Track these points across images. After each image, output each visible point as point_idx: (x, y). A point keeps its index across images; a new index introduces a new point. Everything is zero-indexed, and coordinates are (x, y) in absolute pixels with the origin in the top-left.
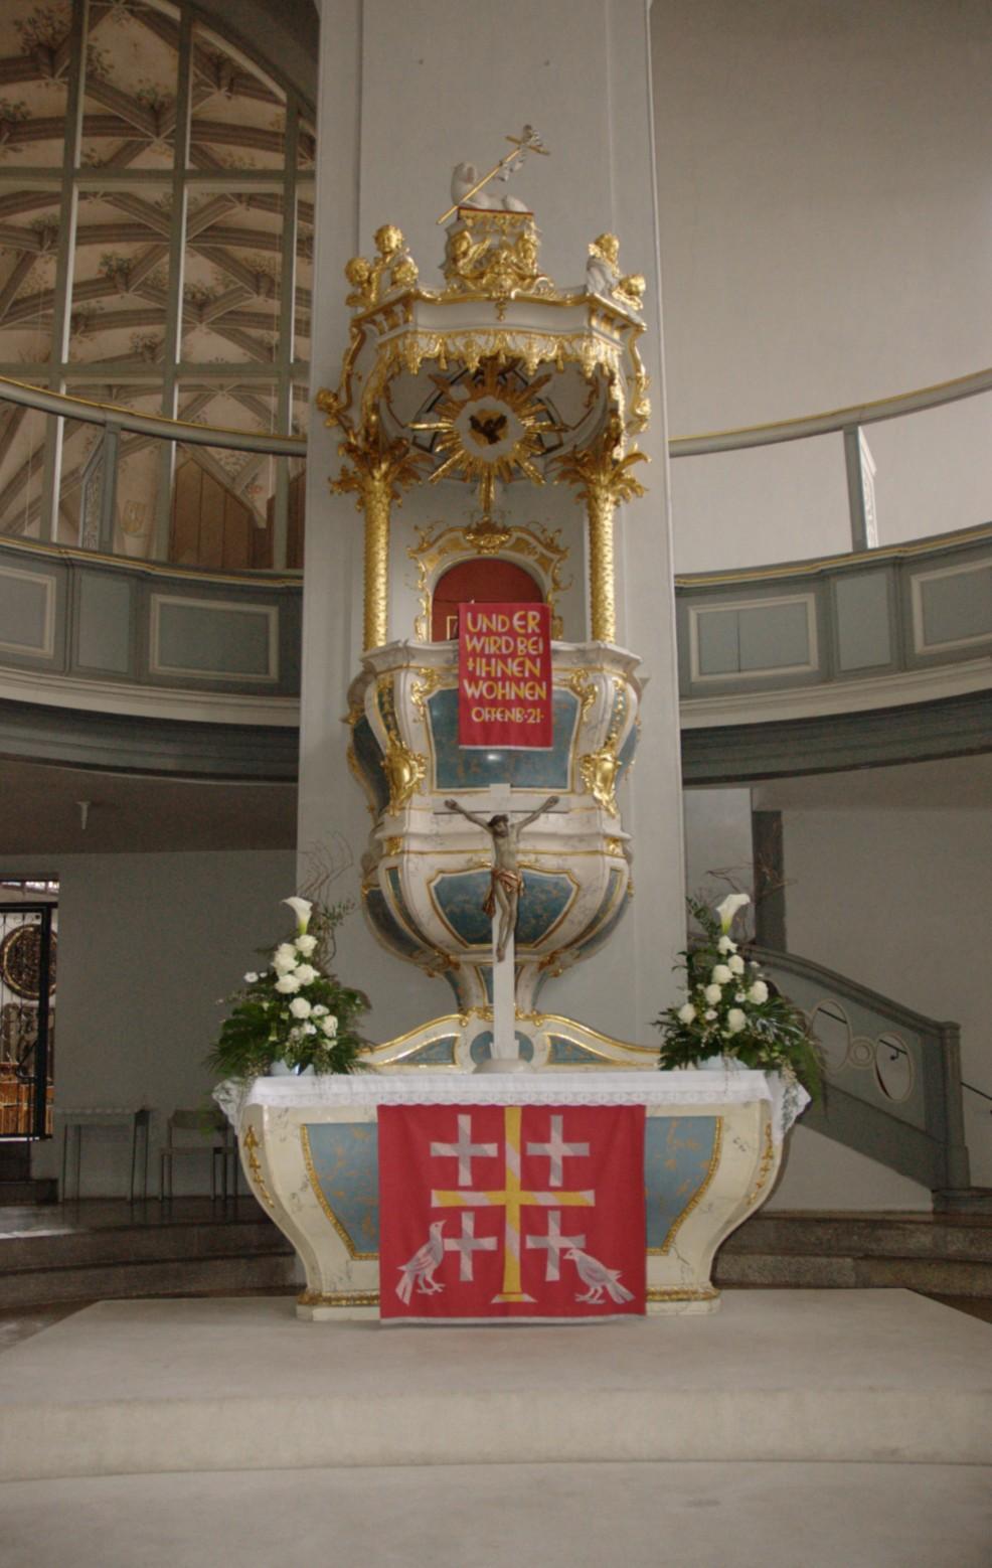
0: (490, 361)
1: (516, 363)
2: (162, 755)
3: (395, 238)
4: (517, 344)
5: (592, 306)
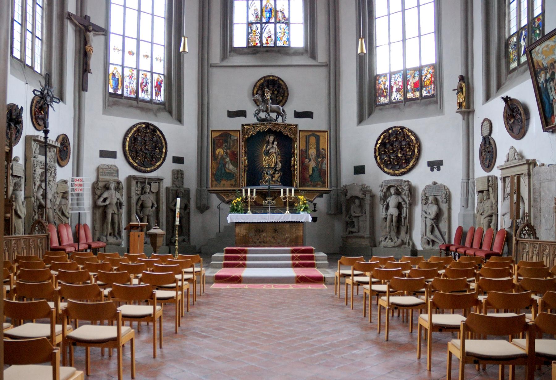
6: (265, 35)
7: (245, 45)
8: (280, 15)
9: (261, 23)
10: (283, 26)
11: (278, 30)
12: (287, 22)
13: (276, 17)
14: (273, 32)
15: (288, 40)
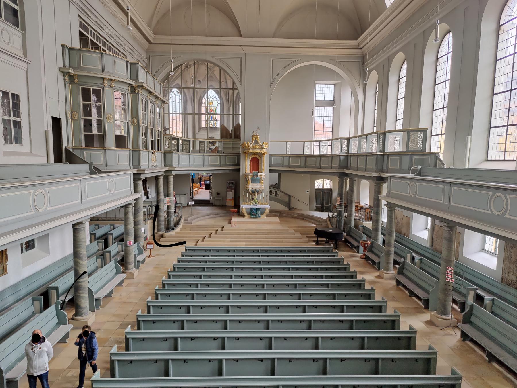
0: (255, 152)
1: (257, 152)
2: (228, 172)
3: (249, 142)
6: (210, 124)
7: (205, 127)
8: (215, 118)
9: (209, 120)
10: (215, 121)
11: (214, 123)
12: (217, 120)
13: (213, 119)
14: (213, 123)
15: (217, 125)
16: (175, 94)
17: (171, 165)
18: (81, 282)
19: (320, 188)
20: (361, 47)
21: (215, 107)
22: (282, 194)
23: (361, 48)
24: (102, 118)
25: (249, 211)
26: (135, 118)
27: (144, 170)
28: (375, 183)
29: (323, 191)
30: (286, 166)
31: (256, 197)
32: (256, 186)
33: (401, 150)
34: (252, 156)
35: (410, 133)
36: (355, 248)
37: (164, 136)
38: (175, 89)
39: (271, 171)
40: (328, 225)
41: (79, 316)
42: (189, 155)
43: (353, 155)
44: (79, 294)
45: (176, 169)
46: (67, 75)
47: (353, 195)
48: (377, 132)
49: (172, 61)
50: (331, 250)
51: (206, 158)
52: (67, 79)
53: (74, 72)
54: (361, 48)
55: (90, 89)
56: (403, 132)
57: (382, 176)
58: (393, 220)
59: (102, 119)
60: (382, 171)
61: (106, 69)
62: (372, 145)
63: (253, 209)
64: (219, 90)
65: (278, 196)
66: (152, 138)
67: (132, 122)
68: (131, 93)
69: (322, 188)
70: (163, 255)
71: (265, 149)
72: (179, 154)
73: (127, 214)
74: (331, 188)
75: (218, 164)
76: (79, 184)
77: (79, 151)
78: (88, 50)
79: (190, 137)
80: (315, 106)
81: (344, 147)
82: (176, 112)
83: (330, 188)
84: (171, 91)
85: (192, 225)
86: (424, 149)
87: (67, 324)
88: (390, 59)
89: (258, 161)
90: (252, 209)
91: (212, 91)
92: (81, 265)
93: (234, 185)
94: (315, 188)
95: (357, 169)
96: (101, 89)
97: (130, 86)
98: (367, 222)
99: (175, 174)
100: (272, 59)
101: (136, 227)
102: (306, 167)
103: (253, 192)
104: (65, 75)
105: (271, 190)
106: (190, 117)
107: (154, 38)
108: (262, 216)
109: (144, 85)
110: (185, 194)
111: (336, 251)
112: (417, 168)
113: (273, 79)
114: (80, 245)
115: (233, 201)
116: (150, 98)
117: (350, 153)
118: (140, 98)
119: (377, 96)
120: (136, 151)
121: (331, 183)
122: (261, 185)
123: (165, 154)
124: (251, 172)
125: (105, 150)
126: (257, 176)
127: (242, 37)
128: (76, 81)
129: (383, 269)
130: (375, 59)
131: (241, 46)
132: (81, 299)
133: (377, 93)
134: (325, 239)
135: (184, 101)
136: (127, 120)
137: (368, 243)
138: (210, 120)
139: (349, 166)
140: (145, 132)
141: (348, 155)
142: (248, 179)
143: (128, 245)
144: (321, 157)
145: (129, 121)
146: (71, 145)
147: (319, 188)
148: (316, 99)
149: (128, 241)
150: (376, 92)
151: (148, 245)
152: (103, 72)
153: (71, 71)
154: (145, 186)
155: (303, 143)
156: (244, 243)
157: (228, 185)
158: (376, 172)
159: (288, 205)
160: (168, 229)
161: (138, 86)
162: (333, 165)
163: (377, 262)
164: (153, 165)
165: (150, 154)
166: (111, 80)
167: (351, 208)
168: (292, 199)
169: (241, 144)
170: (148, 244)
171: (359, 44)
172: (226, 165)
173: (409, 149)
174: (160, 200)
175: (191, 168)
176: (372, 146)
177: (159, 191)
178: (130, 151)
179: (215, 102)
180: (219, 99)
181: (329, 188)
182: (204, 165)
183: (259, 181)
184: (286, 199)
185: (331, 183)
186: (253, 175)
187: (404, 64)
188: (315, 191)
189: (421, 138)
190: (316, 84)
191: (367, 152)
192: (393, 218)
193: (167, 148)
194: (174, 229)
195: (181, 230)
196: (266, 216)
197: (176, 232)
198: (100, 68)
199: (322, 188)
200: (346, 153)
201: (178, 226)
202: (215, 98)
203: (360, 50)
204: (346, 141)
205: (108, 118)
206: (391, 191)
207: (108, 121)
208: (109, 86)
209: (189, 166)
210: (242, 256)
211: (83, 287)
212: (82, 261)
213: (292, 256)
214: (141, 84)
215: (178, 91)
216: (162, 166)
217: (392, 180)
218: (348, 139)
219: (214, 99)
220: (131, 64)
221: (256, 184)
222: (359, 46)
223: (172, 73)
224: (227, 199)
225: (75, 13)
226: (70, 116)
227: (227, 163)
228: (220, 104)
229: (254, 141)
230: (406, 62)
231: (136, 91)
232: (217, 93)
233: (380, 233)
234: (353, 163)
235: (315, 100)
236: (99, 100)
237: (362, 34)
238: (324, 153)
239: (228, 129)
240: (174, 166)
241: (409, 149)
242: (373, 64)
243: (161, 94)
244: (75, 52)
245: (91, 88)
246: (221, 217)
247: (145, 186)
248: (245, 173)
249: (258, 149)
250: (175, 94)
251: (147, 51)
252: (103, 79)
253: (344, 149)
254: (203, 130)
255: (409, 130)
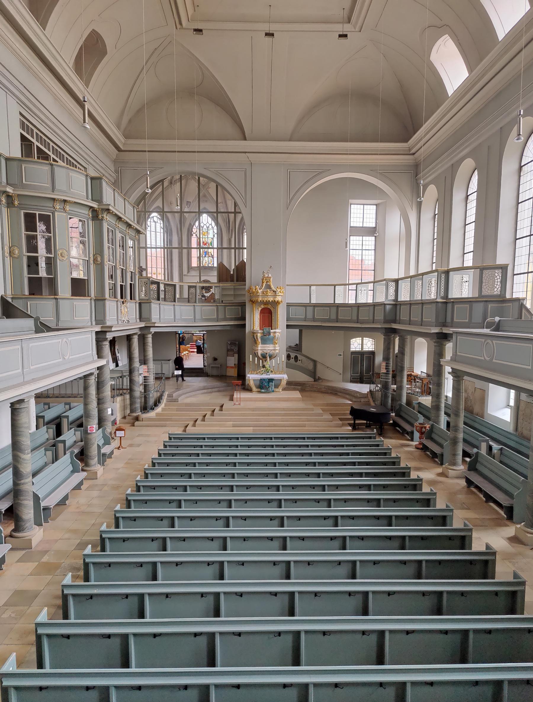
0: (266, 301)
1: (269, 301)
2: (228, 328)
3: (257, 287)
4: (269, 299)
5: (277, 296)
6: (204, 262)
7: (196, 266)
8: (210, 254)
9: (203, 257)
10: (211, 258)
11: (209, 260)
12: (213, 257)
13: (208, 254)
14: (207, 261)
15: (213, 264)
16: (154, 221)
17: (149, 319)
18: (23, 484)
19: (358, 350)
20: (413, 151)
21: (211, 239)
22: (303, 358)
23: (414, 154)
24: (52, 254)
25: (258, 383)
26: (98, 254)
27: (111, 327)
28: (435, 342)
29: (362, 354)
30: (309, 320)
31: (268, 364)
32: (269, 348)
33: (471, 296)
34: (263, 306)
35: (484, 271)
36: (408, 433)
37: (138, 279)
38: (154, 214)
39: (288, 326)
40: (369, 401)
41: (20, 531)
42: (174, 305)
43: (404, 303)
44: (19, 501)
45: (156, 325)
46: (4, 196)
47: (405, 360)
48: (438, 270)
49: (148, 173)
50: (374, 437)
51: (198, 309)
52: (4, 201)
53: (13, 190)
54: (414, 154)
55: (36, 214)
56: (473, 270)
57: (444, 331)
58: (462, 394)
59: (52, 256)
60: (444, 324)
61: (58, 186)
62: (429, 288)
63: (264, 380)
64: (215, 214)
65: (298, 361)
66: (123, 282)
67: (94, 259)
68: (93, 220)
69: (360, 350)
70: (139, 445)
71: (280, 296)
72: (160, 304)
73: (88, 388)
74: (374, 350)
75: (215, 317)
76: (19, 347)
77: (21, 301)
78: (33, 160)
79: (176, 280)
80: (350, 236)
81: (392, 292)
82: (156, 245)
83: (371, 350)
84: (149, 217)
85: (179, 403)
86: (503, 293)
87: (3, 544)
88: (454, 168)
89: (270, 312)
90: (262, 380)
91: (207, 215)
92: (22, 461)
93: (237, 347)
94: (351, 350)
95: (410, 323)
96: (51, 214)
97: (91, 210)
98: (425, 398)
99: (155, 332)
100: (288, 170)
101: (100, 406)
102: (337, 321)
103: (264, 357)
104: (1, 195)
105: (289, 354)
106: (176, 252)
107: (124, 144)
108: (277, 390)
109: (111, 208)
110: (169, 360)
111: (381, 439)
112: (494, 320)
113: (290, 198)
114: (21, 431)
115: (236, 369)
116: (119, 227)
117: (399, 300)
118: (105, 226)
119: (436, 220)
120: (100, 300)
121: (374, 343)
122: (275, 347)
123: (140, 304)
124: (260, 329)
125: (56, 299)
126: (269, 333)
127: (246, 140)
128: (16, 203)
129: (447, 464)
130: (433, 168)
131: (245, 152)
132: (22, 508)
133: (437, 216)
134: (365, 422)
135: (168, 231)
136: (87, 257)
137: (425, 427)
138: (204, 256)
139: (398, 318)
140: (112, 274)
141: (397, 303)
142: (257, 338)
143: (89, 432)
144: (358, 306)
145: (89, 258)
146: (9, 292)
147: (357, 350)
148: (352, 225)
149: (89, 427)
150: (436, 215)
151: (117, 432)
152: (53, 189)
153: (9, 190)
154: (113, 349)
155: (334, 286)
156: (252, 428)
157: (228, 347)
158: (435, 327)
159: (313, 374)
160: (145, 409)
161: (102, 209)
162: (375, 318)
163: (438, 454)
164: (123, 319)
165: (119, 304)
166: (65, 201)
167: (402, 377)
168: (319, 367)
169: (246, 289)
170: (117, 430)
171: (410, 148)
172: (225, 319)
173: (483, 294)
174: (134, 368)
175: (177, 324)
176: (430, 290)
177: (133, 356)
178: (91, 300)
179: (211, 232)
180: (215, 228)
181: (370, 350)
182: (195, 320)
183: (273, 341)
184: (311, 366)
185: (374, 342)
186: (263, 333)
187: (474, 174)
188: (351, 355)
189: (500, 278)
190: (351, 204)
191: (423, 299)
192: (462, 391)
193: (143, 295)
194: (153, 409)
195: (163, 410)
196: (283, 390)
197: (156, 413)
198: (49, 185)
199: (360, 350)
200: (394, 300)
201: (160, 405)
202: (210, 226)
203: (411, 157)
204: (393, 284)
205: (61, 255)
206: (458, 353)
207: (61, 258)
208: (62, 210)
209: (175, 321)
210: (249, 446)
211: (27, 491)
212: (24, 454)
213: (320, 446)
214: (106, 207)
215: (158, 216)
216: (136, 321)
217: (458, 337)
218: (397, 281)
219: (209, 227)
220: (92, 179)
221: (268, 346)
222: (410, 150)
223: (148, 190)
224: (227, 367)
225: (15, 109)
226: (8, 252)
227: (227, 317)
228: (217, 234)
229: (264, 285)
230: (476, 172)
231: (100, 216)
232: (212, 219)
233: (442, 413)
234: (403, 315)
235: (350, 227)
236: (48, 230)
237: (415, 134)
238: (363, 300)
239: (229, 269)
240: (153, 321)
241: (483, 294)
242: (430, 175)
243: (134, 220)
244: (15, 163)
245: (37, 213)
246: (219, 391)
247: (113, 349)
248: (252, 329)
249: (270, 296)
250: (154, 221)
251: (115, 162)
252: (54, 199)
253: (391, 294)
254: (195, 270)
255: (482, 267)
